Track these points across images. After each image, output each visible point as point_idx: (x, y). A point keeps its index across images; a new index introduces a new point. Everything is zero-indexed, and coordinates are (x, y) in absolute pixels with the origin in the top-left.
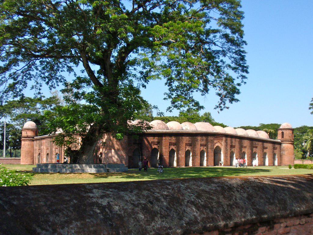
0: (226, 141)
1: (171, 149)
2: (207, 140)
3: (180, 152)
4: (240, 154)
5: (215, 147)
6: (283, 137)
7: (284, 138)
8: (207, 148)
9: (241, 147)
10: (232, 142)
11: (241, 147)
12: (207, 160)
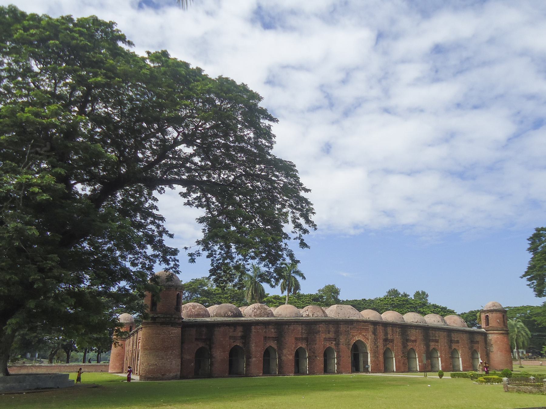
0: (374, 333)
1: (268, 345)
2: (337, 333)
3: (285, 352)
4: (403, 353)
5: (353, 342)
6: (487, 323)
7: (490, 325)
8: (337, 344)
9: (405, 341)
10: (386, 334)
11: (405, 341)
12: (338, 364)
